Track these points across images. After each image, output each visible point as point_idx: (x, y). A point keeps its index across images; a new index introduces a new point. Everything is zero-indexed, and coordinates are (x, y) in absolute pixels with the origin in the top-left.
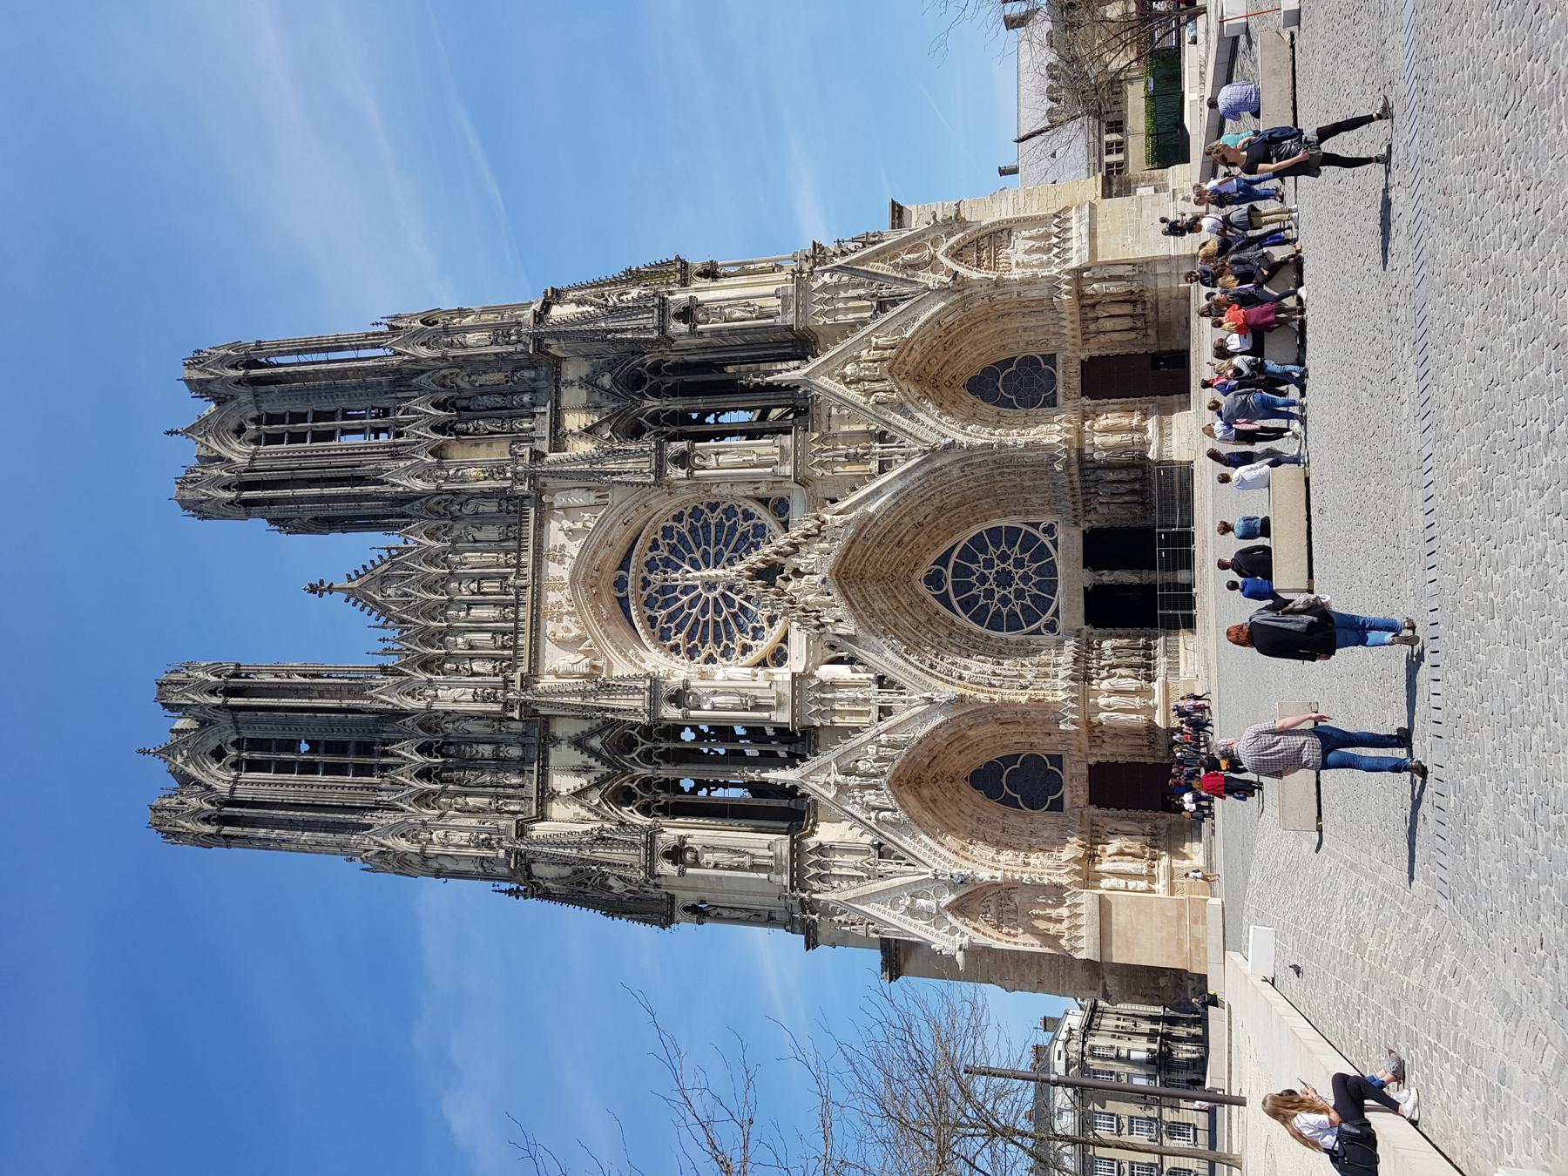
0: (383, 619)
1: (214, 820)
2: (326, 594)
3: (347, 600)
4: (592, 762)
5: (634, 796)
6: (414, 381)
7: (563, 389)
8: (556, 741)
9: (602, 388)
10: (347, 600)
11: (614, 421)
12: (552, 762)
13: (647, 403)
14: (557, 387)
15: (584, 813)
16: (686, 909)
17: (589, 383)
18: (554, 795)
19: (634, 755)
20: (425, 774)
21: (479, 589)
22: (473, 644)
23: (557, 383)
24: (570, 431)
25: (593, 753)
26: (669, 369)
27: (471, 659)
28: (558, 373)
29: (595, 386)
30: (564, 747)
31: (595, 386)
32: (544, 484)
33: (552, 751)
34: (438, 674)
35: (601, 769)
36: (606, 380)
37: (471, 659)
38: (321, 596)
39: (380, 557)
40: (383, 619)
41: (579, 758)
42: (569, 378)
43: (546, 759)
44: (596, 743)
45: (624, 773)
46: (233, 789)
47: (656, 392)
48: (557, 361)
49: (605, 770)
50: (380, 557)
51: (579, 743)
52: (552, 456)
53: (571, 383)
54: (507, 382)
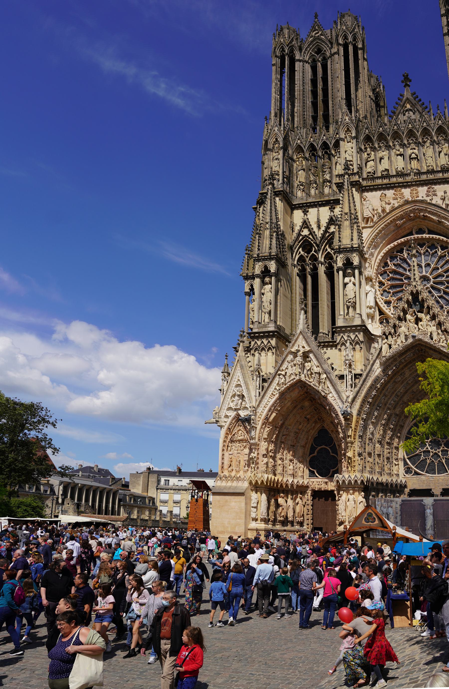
1: (283, 53)
4: (323, 228)
12: (321, 209)
15: (297, 228)
18: (305, 212)
20: (312, 148)
21: (412, 158)
22: (382, 160)
25: (328, 228)
33: (327, 208)
41: (324, 222)
45: (318, 246)
46: (300, 61)
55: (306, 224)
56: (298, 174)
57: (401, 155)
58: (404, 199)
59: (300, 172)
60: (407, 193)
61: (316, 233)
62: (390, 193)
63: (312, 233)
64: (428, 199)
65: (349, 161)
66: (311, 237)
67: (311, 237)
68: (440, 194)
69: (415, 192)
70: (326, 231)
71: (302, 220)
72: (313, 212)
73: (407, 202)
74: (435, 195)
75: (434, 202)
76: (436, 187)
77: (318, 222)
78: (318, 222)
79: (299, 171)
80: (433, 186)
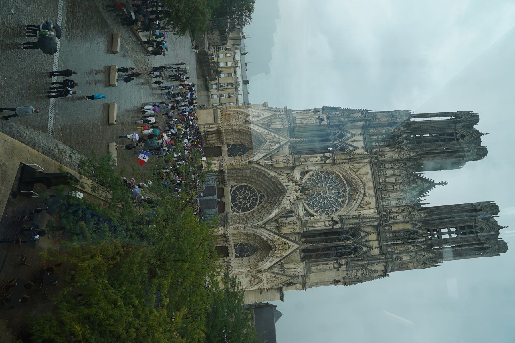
0: (421, 176)
2: (441, 182)
3: (434, 181)
4: (351, 143)
5: (338, 137)
6: (426, 246)
7: (378, 246)
8: (363, 148)
9: (366, 246)
10: (434, 181)
11: (360, 237)
12: (362, 142)
13: (351, 243)
14: (380, 246)
15: (351, 131)
16: (319, 111)
17: (370, 248)
18: (360, 135)
19: (340, 147)
23: (380, 247)
24: (373, 234)
25: (351, 146)
26: (347, 254)
27: (392, 167)
28: (380, 250)
29: (368, 247)
30: (360, 147)
31: (368, 247)
32: (377, 215)
34: (401, 162)
35: (348, 142)
36: (365, 249)
37: (392, 167)
38: (442, 181)
39: (426, 194)
40: (421, 176)
41: (355, 144)
42: (376, 249)
43: (364, 143)
44: (351, 148)
45: (341, 142)
47: (349, 247)
48: (381, 254)
49: (347, 142)
50: (426, 194)
51: (356, 148)
52: (376, 223)
53: (375, 248)
54: (396, 248)
55: (354, 135)
56: (383, 130)
57: (396, 181)
58: (366, 183)
59: (384, 130)
60: (370, 184)
61: (348, 140)
62: (370, 176)
63: (348, 139)
64: (367, 195)
65: (387, 156)
66: (346, 138)
67: (346, 138)
68: (370, 201)
69: (370, 188)
70: (349, 145)
71: (355, 133)
72: (361, 138)
73: (364, 185)
74: (369, 198)
75: (365, 198)
76: (374, 199)
77: (355, 141)
78: (355, 141)
79: (385, 130)
80: (374, 197)
